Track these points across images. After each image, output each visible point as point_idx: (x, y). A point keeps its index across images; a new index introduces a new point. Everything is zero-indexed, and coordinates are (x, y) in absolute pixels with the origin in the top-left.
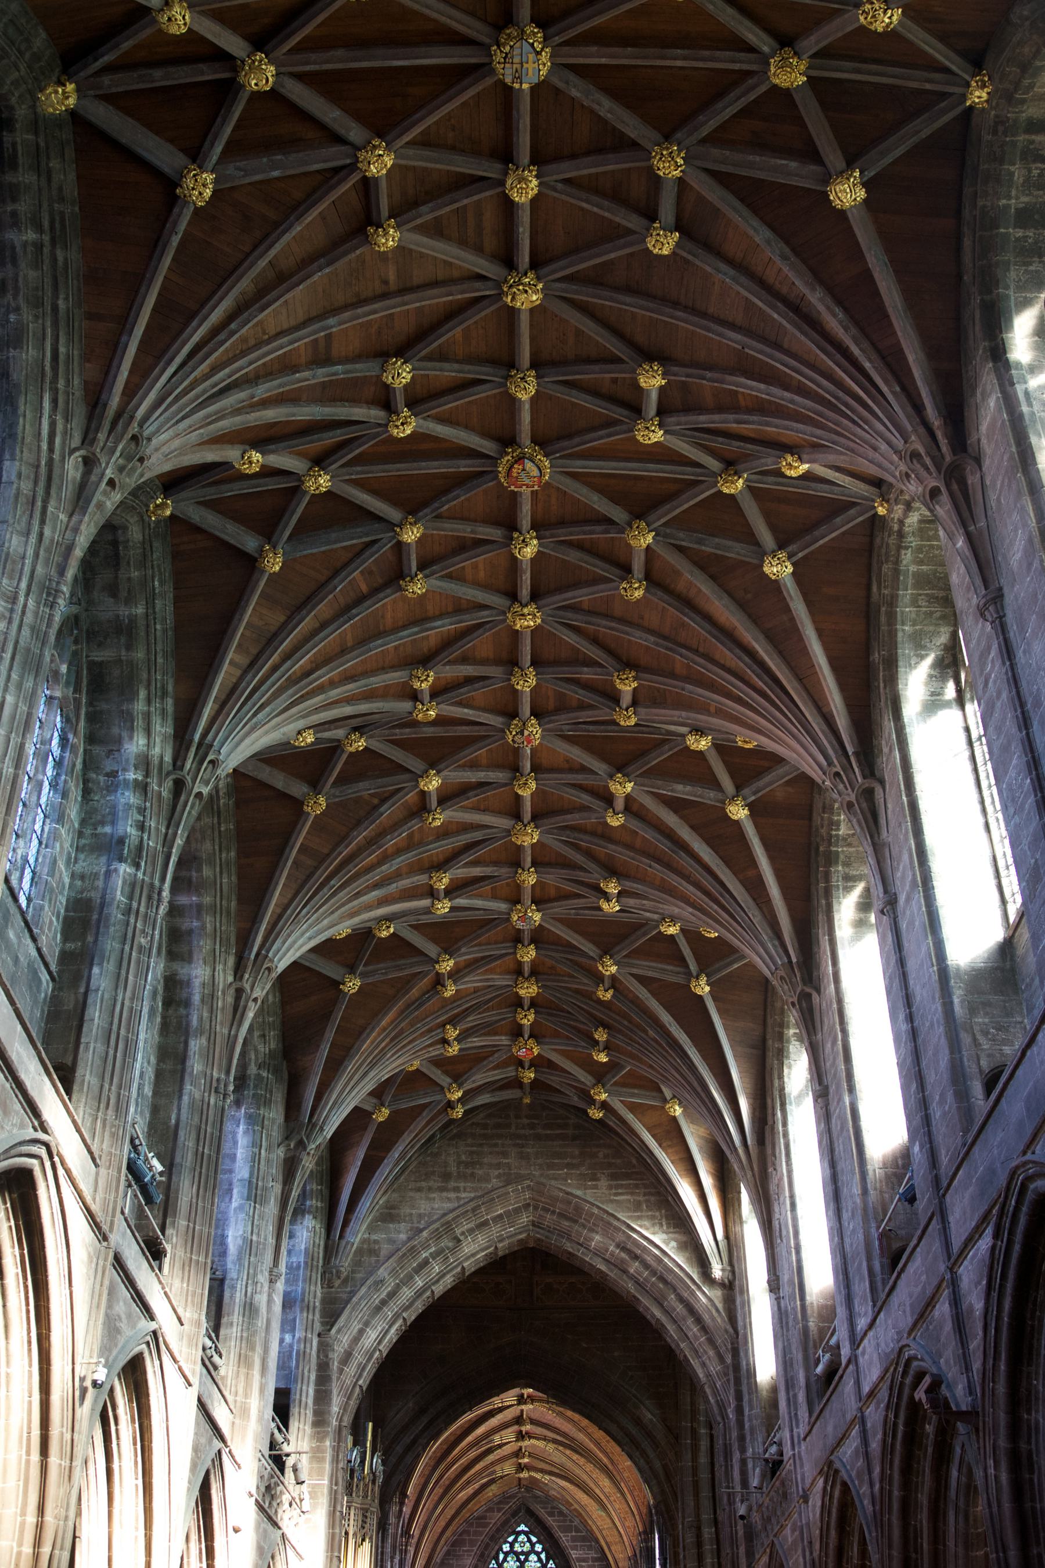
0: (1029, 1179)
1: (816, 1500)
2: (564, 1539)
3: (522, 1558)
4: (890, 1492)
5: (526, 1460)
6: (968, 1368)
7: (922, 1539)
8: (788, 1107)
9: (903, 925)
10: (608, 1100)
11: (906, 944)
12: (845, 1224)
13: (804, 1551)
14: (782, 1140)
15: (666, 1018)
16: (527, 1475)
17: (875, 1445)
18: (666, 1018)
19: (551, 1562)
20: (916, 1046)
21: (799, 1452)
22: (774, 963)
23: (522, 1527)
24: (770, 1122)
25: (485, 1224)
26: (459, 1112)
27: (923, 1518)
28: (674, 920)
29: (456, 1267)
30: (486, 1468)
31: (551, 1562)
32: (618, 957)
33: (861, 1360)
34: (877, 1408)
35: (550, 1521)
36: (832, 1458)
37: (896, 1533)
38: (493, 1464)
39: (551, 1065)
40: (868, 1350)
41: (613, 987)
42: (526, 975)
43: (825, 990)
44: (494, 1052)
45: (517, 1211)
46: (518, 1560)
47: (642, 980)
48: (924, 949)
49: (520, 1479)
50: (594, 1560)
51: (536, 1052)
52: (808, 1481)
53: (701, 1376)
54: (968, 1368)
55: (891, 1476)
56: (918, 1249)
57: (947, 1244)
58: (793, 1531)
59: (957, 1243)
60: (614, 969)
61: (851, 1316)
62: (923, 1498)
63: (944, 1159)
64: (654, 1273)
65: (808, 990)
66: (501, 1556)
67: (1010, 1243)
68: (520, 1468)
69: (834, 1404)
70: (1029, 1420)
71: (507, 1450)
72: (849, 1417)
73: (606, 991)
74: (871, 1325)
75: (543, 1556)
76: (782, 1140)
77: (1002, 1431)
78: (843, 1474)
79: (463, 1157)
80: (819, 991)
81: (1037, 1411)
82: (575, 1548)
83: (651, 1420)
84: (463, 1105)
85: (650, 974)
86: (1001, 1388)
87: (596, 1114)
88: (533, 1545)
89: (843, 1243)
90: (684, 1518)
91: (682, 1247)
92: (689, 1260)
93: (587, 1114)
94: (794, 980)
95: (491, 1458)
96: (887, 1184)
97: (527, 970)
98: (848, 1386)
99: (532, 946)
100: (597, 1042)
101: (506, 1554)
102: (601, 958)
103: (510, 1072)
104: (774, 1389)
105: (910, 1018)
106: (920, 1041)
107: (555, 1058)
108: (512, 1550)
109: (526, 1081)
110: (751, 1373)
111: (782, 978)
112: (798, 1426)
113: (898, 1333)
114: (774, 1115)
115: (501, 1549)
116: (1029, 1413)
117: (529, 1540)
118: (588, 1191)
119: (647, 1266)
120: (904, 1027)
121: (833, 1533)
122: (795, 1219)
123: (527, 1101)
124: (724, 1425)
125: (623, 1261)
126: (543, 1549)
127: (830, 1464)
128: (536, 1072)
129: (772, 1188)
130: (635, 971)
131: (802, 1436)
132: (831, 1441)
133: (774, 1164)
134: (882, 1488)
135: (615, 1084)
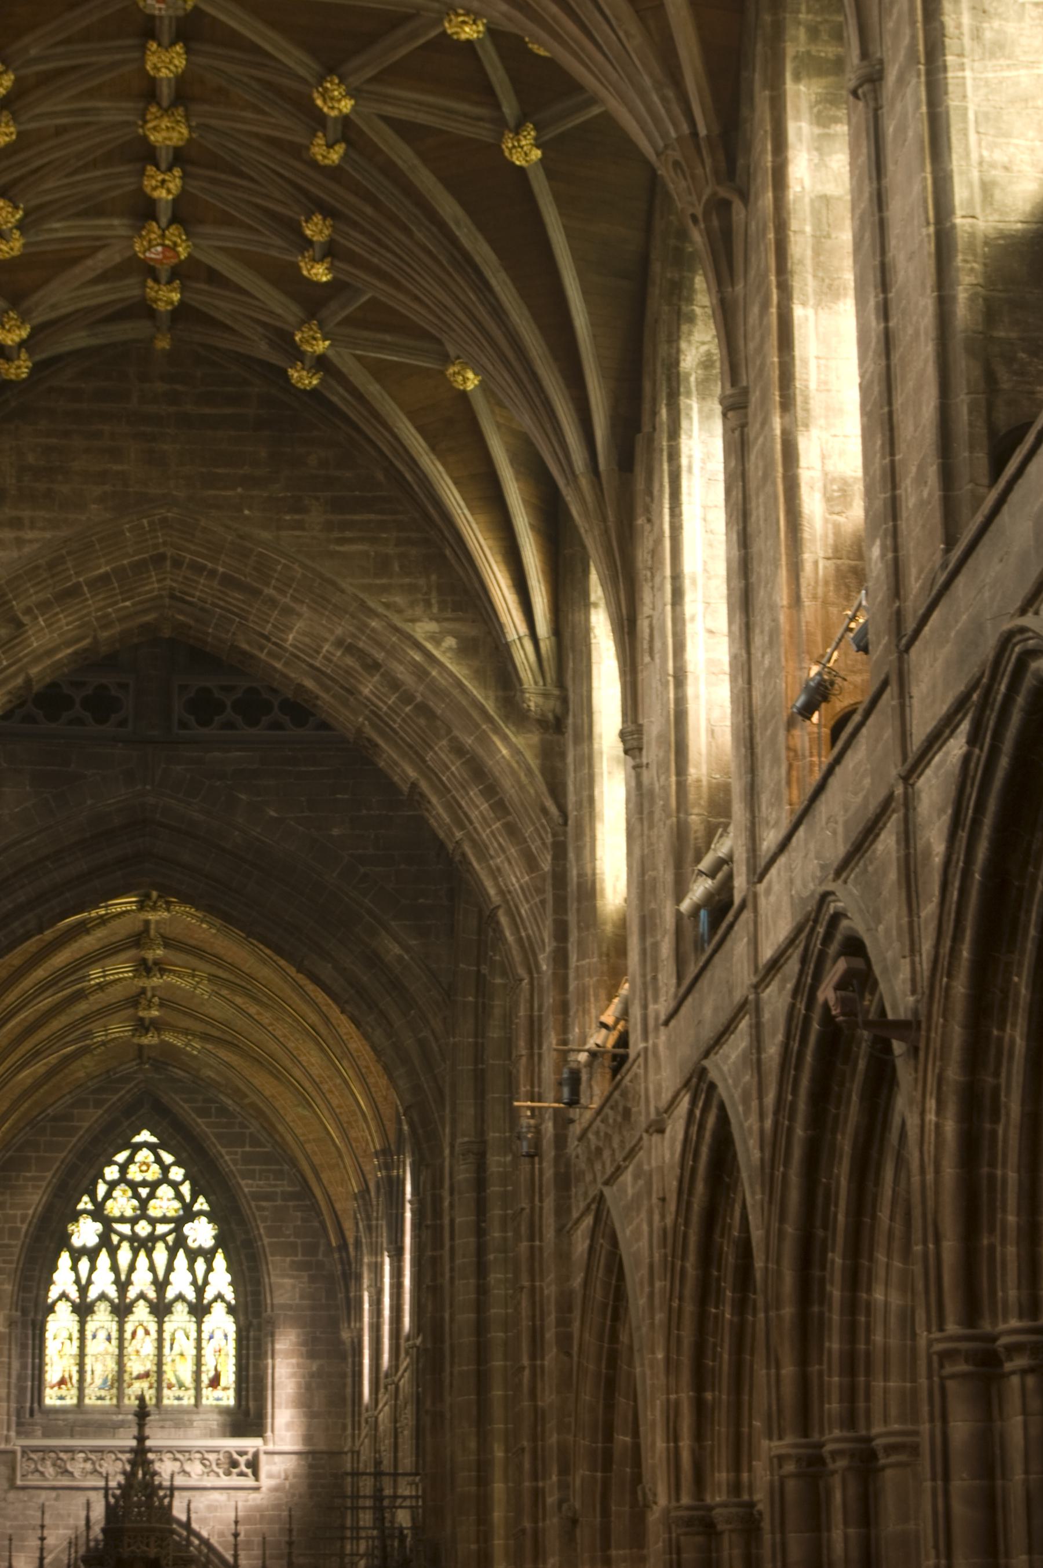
0: (1030, 654)
1: (676, 1128)
2: (228, 1158)
3: (144, 1192)
4: (790, 1130)
5: (155, 1013)
6: (914, 949)
7: (836, 1205)
8: (683, 401)
9: (890, 129)
10: (331, 353)
11: (891, 167)
12: (757, 654)
13: (650, 1212)
14: (666, 466)
15: (449, 208)
16: (155, 1041)
17: (772, 1050)
18: (449, 208)
19: (201, 1199)
20: (888, 367)
21: (655, 1046)
22: (664, 135)
23: (145, 1136)
24: (646, 428)
25: (74, 592)
26: (21, 368)
27: (843, 1172)
28: (476, 16)
29: (15, 675)
30: (73, 1026)
31: (201, 1199)
32: (355, 81)
33: (762, 901)
34: (781, 989)
35: (201, 1125)
36: (706, 1063)
37: (794, 1196)
38: (86, 1018)
39: (213, 276)
40: (776, 888)
41: (345, 138)
42: (165, 103)
43: (757, 198)
44: (96, 249)
45: (139, 567)
46: (136, 1195)
47: (405, 130)
48: (917, 188)
49: (141, 1047)
50: (287, 1196)
51: (183, 252)
52: (666, 1096)
53: (492, 892)
54: (914, 949)
55: (793, 1105)
56: (864, 731)
57: (904, 735)
58: (636, 1177)
59: (919, 733)
60: (346, 105)
61: (753, 824)
62: (845, 1143)
63: (915, 585)
64: (407, 698)
65: (723, 193)
66: (102, 1189)
67: (994, 752)
68: (142, 1026)
69: (717, 972)
70: (1000, 1039)
71: (115, 994)
72: (738, 997)
73: (330, 146)
74: (784, 846)
75: (186, 1189)
76: (666, 466)
77: (955, 1054)
78: (721, 1089)
79: (31, 459)
80: (745, 196)
81: (1014, 1025)
82: (249, 1175)
83: (400, 959)
84: (31, 353)
85: (422, 118)
86: (960, 988)
87: (304, 378)
88: (165, 1169)
89: (750, 690)
90: (453, 1136)
91: (466, 649)
92: (479, 675)
93: (287, 378)
94: (699, 171)
95: (82, 1007)
96: (837, 588)
97: (166, 93)
98: (739, 945)
99: (179, 48)
100: (309, 243)
101: (112, 1185)
102: (321, 80)
103: (128, 289)
104: (623, 924)
105: (885, 311)
106: (895, 358)
107: (223, 265)
108: (123, 1179)
109: (161, 306)
110: (589, 891)
111: (676, 164)
112: (656, 1000)
113: (823, 867)
114: (654, 413)
115: (102, 1177)
116: (1002, 1028)
117: (158, 1160)
118: (284, 533)
119: (395, 685)
120: (875, 325)
121: (700, 1187)
122: (679, 621)
123: (163, 343)
124: (531, 983)
125: (348, 672)
126: (186, 1177)
127: (703, 1072)
128: (183, 290)
129: (642, 556)
130: (390, 110)
131: (663, 1017)
132: (708, 1033)
133: (648, 510)
134: (776, 1124)
135: (347, 321)
